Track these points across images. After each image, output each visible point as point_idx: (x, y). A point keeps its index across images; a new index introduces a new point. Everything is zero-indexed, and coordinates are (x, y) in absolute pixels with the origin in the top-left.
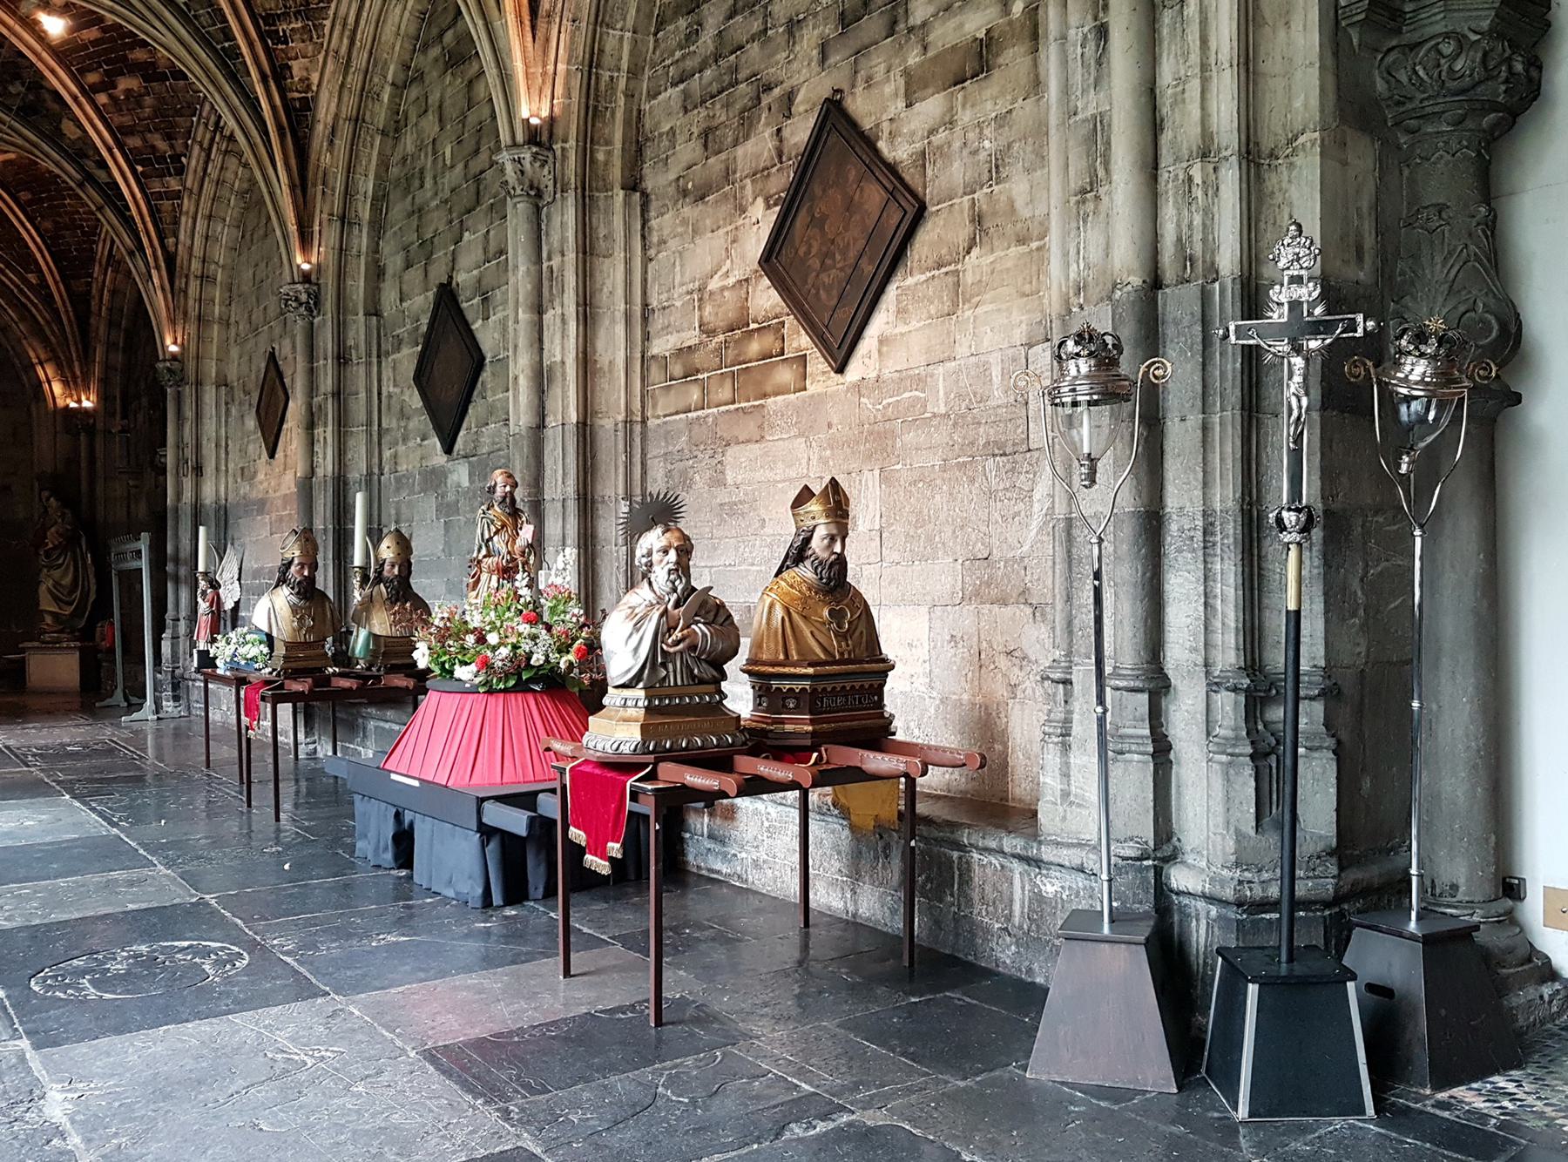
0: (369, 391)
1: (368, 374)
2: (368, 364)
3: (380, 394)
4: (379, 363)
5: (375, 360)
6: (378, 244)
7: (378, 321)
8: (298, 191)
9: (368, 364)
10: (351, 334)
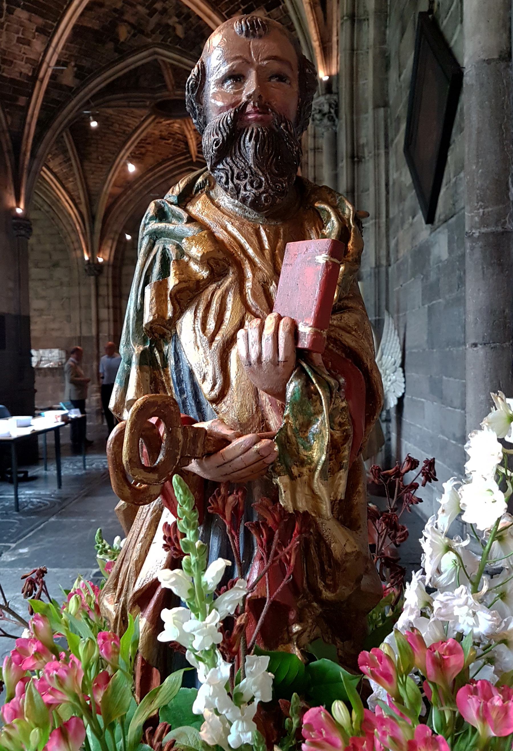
0: (377, 183)
1: (377, 166)
2: (377, 156)
3: (387, 185)
4: (387, 154)
5: (382, 151)
6: (385, 34)
7: (386, 112)
8: (319, 9)
9: (377, 156)
10: (363, 133)
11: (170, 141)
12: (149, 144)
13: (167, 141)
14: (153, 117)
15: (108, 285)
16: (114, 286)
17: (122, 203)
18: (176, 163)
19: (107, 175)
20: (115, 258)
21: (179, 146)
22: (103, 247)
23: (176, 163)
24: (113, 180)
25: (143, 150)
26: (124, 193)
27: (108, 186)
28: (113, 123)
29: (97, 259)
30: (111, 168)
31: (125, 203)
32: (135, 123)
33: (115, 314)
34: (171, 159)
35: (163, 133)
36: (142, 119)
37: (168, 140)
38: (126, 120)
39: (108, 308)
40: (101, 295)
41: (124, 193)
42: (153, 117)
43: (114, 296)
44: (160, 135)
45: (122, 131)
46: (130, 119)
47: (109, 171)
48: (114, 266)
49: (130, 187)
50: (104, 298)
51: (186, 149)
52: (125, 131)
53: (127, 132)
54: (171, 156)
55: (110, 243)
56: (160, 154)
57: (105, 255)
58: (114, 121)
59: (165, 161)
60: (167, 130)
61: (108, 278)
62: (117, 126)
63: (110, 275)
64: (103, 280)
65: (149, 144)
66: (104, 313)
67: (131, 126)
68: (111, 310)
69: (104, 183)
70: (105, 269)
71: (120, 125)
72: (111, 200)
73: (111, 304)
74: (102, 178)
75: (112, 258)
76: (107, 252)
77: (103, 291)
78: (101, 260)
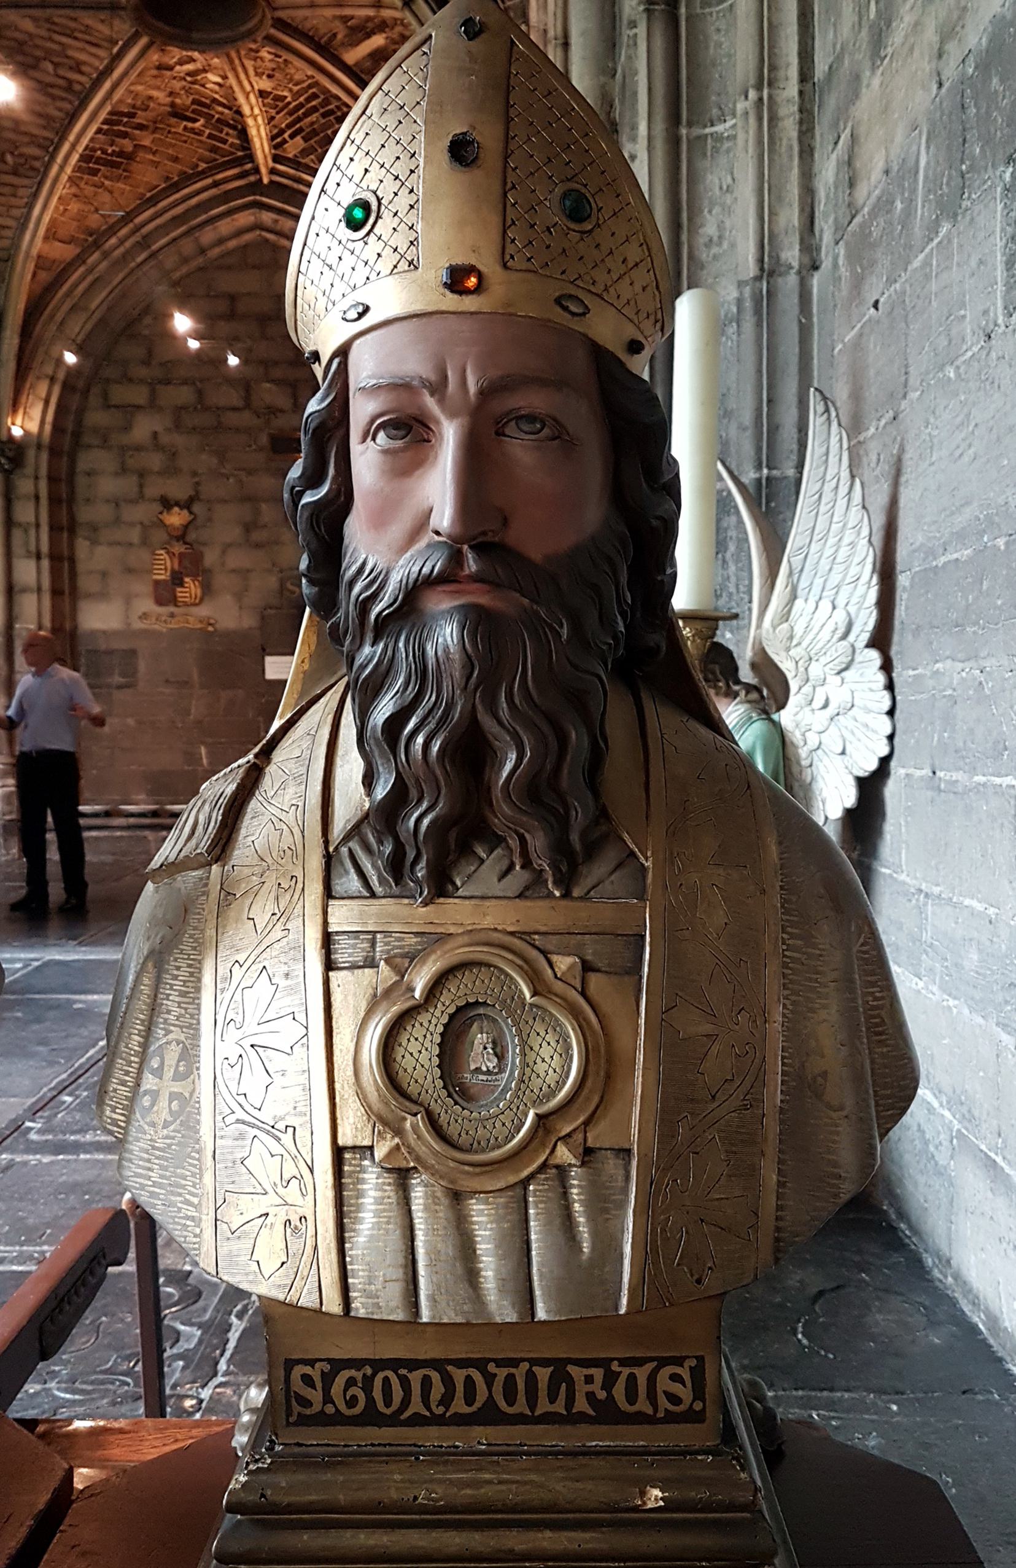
11: (197, 125)
12: (141, 127)
13: (190, 125)
14: (144, 41)
15: (37, 498)
16: (54, 501)
17: (76, 285)
18: (216, 184)
19: (30, 206)
20: (57, 427)
21: (225, 142)
22: (23, 399)
23: (216, 184)
24: (46, 219)
25: (127, 145)
26: (79, 259)
27: (34, 235)
28: (38, 59)
29: (9, 429)
30: (40, 184)
31: (81, 288)
32: (97, 63)
33: (55, 573)
34: (203, 174)
35: (178, 101)
36: (115, 50)
37: (195, 121)
38: (70, 53)
39: (38, 557)
40: (20, 525)
41: (79, 259)
42: (144, 41)
43: (55, 528)
44: (173, 105)
45: (61, 82)
46: (82, 50)
47: (35, 195)
48: (54, 451)
49: (97, 245)
50: (26, 531)
51: (244, 149)
52: (70, 82)
53: (77, 87)
54: (203, 166)
55: (42, 388)
56: (176, 160)
57: (31, 419)
58: (39, 53)
59: (186, 179)
60: (188, 91)
61: (37, 478)
62: (50, 67)
63: (44, 471)
64: (24, 486)
65: (141, 127)
66: (27, 571)
67: (84, 68)
68: (45, 563)
69: (23, 227)
70: (31, 453)
71: (56, 65)
72: (44, 277)
73: (45, 548)
74: (16, 212)
75: (48, 428)
76: (36, 412)
77: (25, 512)
78: (17, 432)
